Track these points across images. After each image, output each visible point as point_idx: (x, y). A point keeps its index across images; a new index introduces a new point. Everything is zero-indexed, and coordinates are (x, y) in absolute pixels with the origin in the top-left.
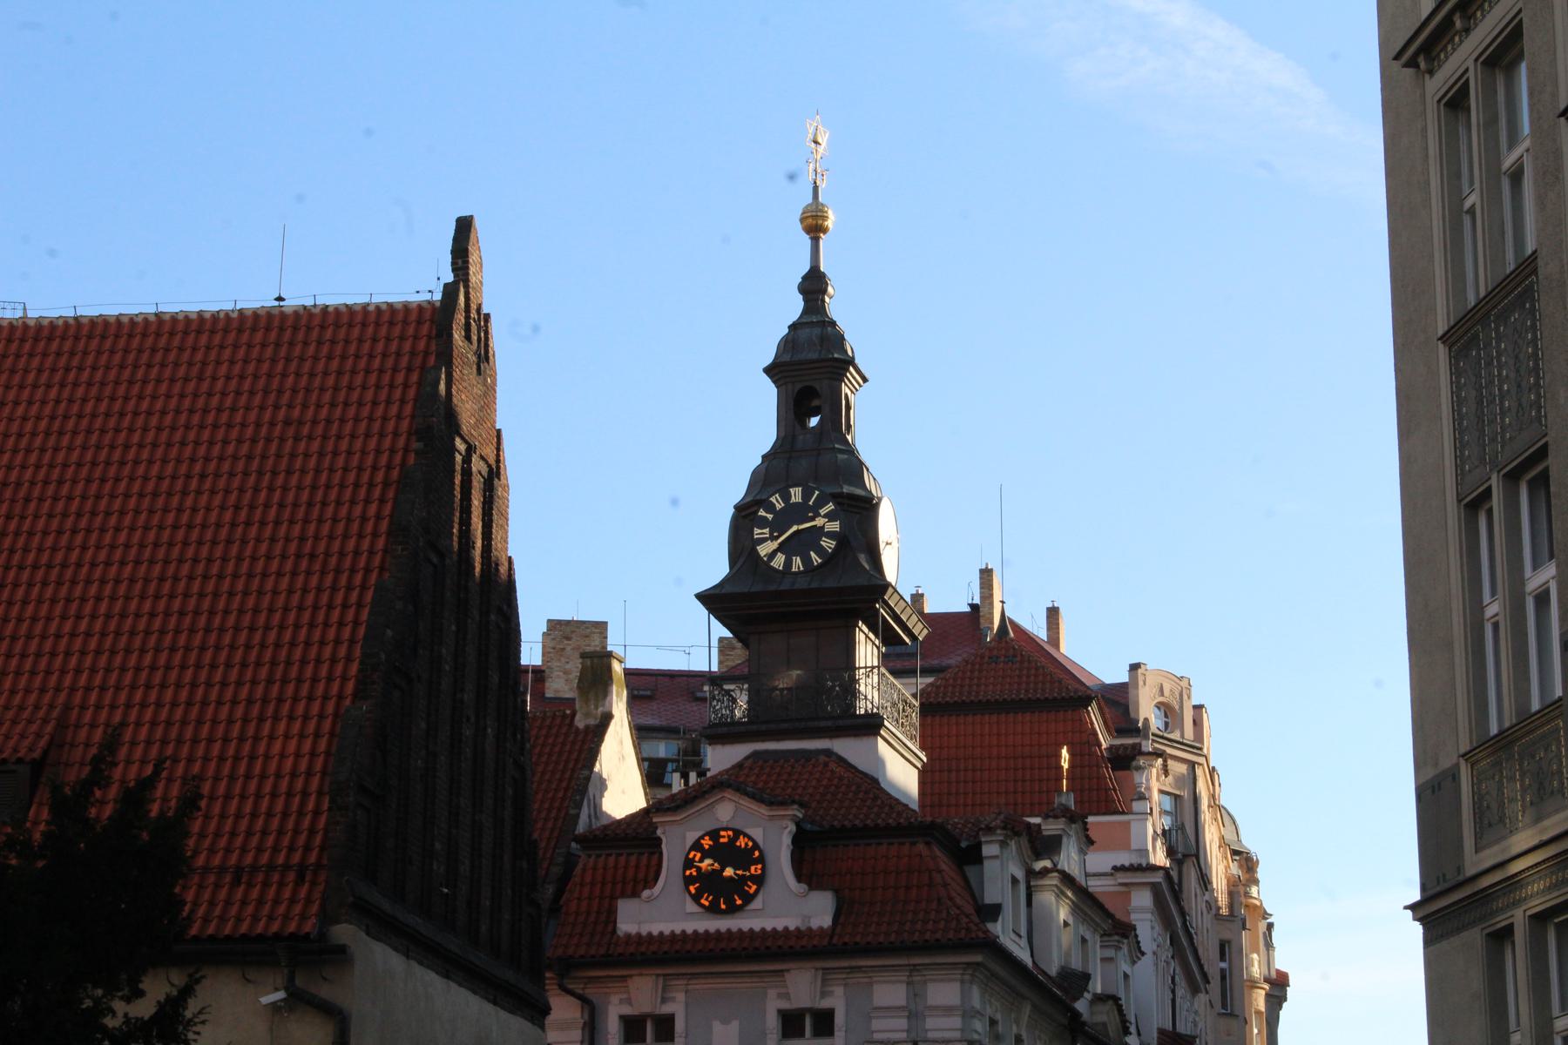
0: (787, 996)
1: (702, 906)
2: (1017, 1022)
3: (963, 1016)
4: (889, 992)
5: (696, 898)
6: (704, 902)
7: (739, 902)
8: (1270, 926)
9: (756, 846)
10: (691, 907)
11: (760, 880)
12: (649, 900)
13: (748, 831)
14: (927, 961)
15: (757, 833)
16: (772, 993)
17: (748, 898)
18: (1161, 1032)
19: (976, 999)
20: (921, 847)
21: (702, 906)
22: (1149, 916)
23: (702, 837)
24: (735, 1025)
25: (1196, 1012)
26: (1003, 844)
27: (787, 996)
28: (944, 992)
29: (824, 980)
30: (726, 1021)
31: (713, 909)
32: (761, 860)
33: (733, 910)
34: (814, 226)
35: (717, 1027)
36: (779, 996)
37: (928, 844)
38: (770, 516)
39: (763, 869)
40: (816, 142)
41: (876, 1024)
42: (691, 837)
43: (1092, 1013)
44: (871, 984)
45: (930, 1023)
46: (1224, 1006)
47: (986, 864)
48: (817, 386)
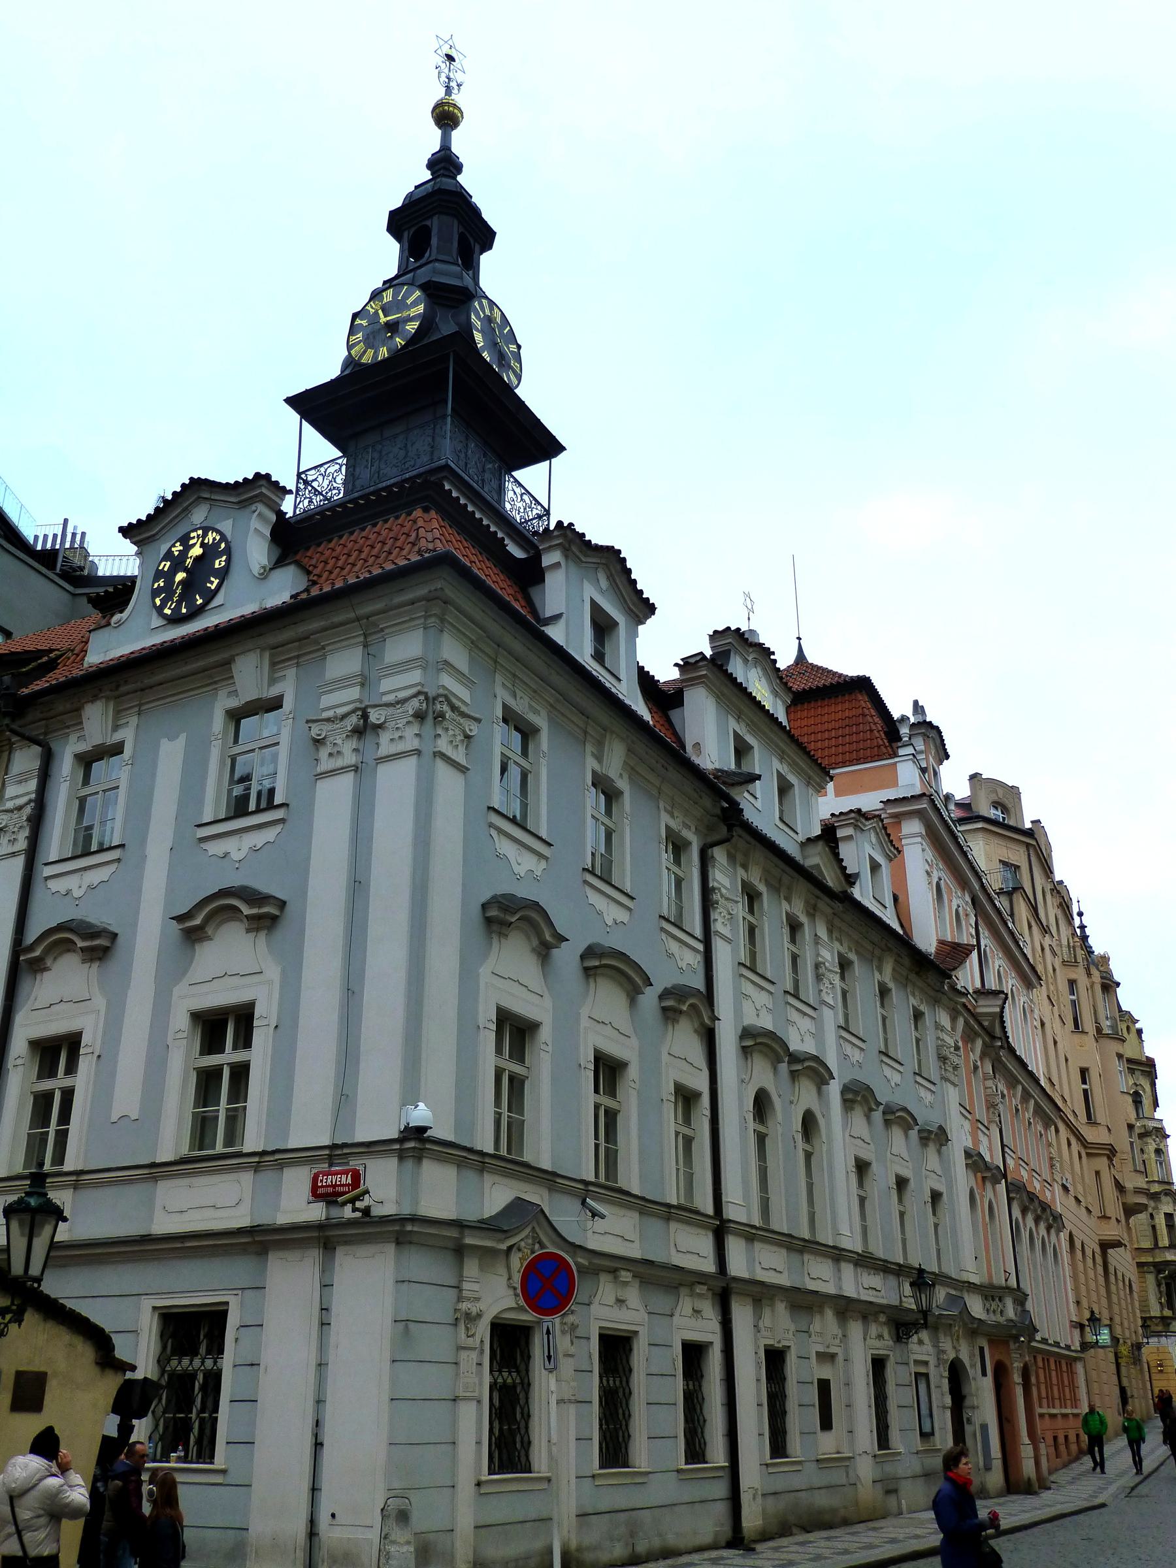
0: (235, 693)
1: (165, 616)
2: (599, 758)
3: (424, 668)
4: (345, 662)
5: (159, 610)
6: (167, 611)
7: (200, 601)
8: (1140, 1032)
9: (223, 538)
10: (157, 621)
11: (223, 574)
12: (120, 624)
13: (218, 527)
14: (379, 606)
15: (226, 526)
16: (222, 694)
17: (211, 595)
18: (941, 942)
19: (453, 651)
20: (418, 513)
21: (165, 616)
22: (919, 839)
23: (174, 546)
24: (182, 740)
25: (1031, 1001)
26: (567, 552)
27: (235, 693)
28: (405, 645)
29: (273, 664)
30: (172, 738)
31: (176, 620)
32: (228, 551)
33: (196, 613)
34: (446, 117)
35: (166, 746)
36: (230, 694)
37: (426, 510)
38: (364, 323)
39: (228, 561)
40: (450, 58)
41: (327, 700)
42: (164, 549)
43: (804, 857)
44: (324, 657)
45: (386, 685)
46: (1076, 1026)
47: (549, 578)
48: (428, 223)
